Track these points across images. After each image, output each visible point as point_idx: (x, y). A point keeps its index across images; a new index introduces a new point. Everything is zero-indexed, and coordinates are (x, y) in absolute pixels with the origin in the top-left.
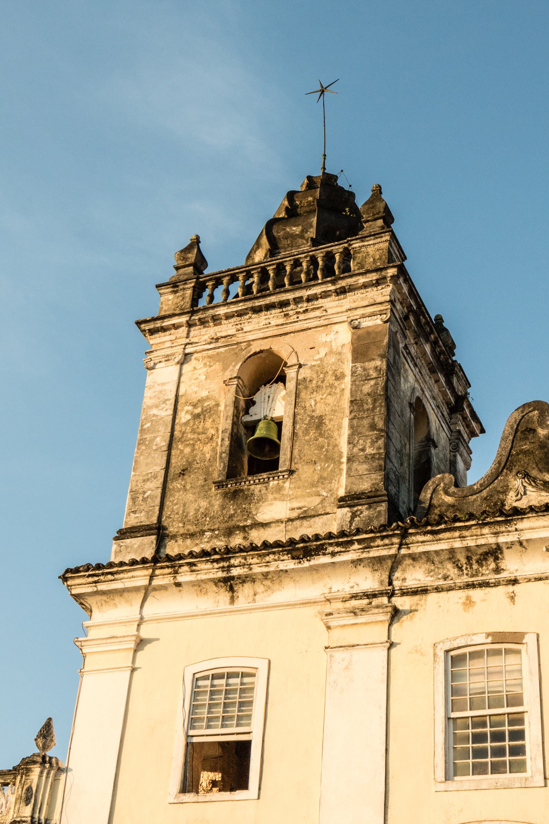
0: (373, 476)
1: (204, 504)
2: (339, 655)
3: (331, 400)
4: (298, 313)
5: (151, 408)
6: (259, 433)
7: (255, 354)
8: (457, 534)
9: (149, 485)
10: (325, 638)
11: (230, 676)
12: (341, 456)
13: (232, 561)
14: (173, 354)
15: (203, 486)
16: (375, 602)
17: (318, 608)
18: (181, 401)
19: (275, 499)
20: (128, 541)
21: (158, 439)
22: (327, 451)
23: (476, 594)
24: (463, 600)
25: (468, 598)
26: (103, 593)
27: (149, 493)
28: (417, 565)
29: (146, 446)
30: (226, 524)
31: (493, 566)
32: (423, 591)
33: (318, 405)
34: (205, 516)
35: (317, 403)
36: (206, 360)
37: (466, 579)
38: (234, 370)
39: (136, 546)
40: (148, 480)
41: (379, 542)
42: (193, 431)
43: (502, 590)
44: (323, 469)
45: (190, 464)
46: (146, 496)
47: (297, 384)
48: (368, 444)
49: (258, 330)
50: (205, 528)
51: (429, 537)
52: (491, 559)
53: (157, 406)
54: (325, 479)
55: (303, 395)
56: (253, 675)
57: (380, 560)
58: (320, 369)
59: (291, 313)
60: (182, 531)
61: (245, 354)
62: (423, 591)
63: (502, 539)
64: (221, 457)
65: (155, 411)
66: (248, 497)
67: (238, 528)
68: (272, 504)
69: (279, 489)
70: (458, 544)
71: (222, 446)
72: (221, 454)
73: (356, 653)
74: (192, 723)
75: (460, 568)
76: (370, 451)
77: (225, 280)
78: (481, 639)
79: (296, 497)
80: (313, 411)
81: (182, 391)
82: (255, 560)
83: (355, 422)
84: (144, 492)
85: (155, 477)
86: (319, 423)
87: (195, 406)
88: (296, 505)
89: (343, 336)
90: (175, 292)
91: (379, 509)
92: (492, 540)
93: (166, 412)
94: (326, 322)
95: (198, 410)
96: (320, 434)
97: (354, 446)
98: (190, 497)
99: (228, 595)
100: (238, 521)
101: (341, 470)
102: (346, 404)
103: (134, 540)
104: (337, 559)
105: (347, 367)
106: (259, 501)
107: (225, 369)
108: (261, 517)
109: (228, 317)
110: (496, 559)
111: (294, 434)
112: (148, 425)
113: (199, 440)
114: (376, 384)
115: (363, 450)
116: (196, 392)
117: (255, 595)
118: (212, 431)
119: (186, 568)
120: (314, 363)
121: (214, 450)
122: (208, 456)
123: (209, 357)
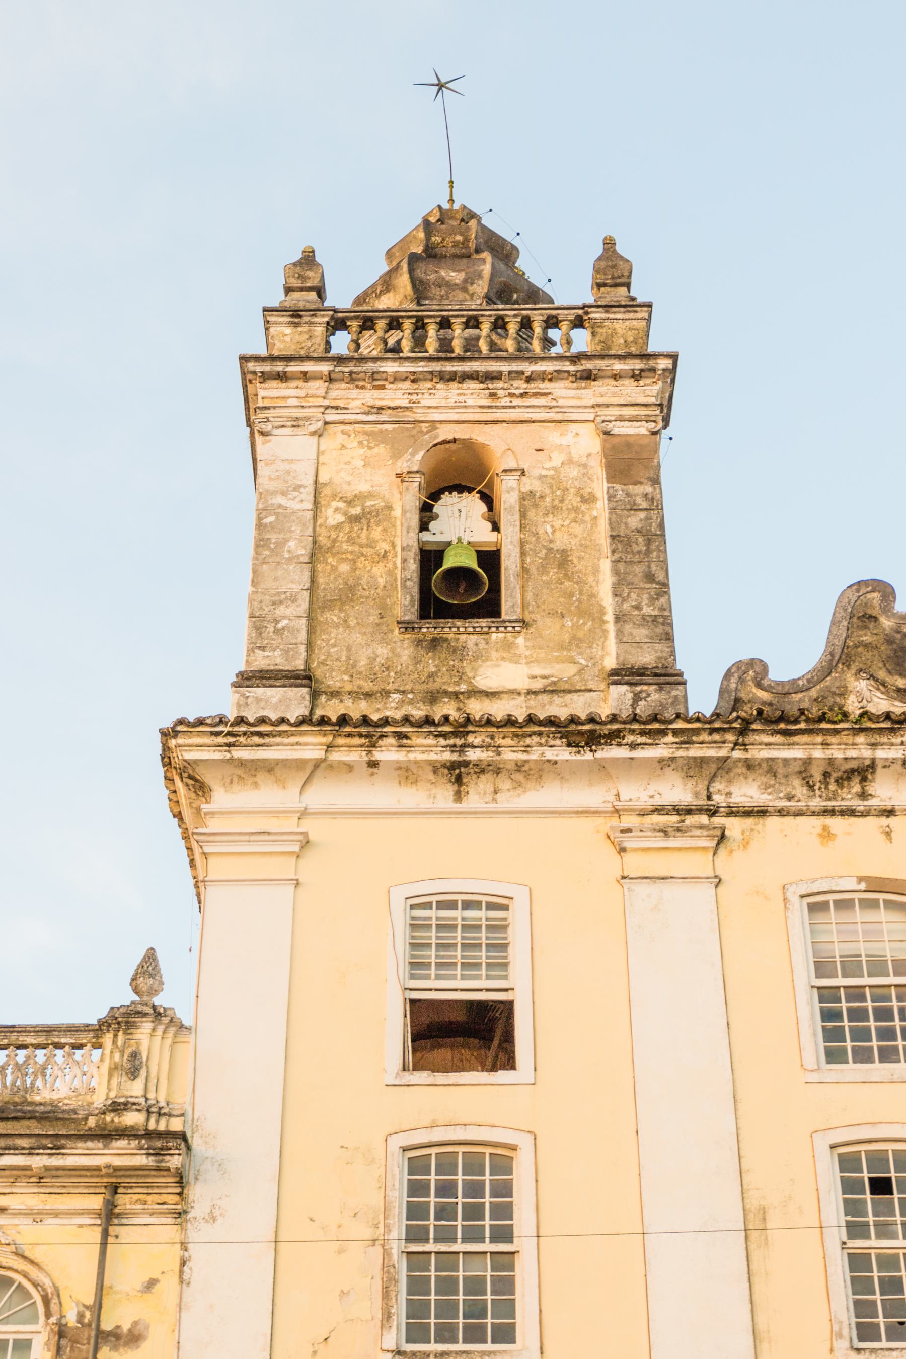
0: (658, 647)
1: (383, 652)
2: (643, 889)
3: (577, 529)
4: (511, 395)
5: (274, 493)
6: (450, 562)
7: (445, 442)
8: (819, 739)
10: (612, 864)
11: (467, 905)
12: (602, 611)
13: (471, 739)
14: (307, 419)
15: (378, 625)
16: (690, 820)
17: (599, 821)
18: (327, 491)
19: (503, 659)
20: (260, 691)
21: (292, 544)
22: (579, 600)
23: (836, 824)
24: (819, 830)
25: (825, 828)
26: (241, 763)
27: (284, 622)
28: (751, 776)
29: (272, 550)
30: (425, 686)
31: (857, 788)
32: (762, 813)
33: (558, 534)
34: (388, 669)
35: (558, 531)
36: (361, 438)
37: (817, 803)
38: (415, 460)
39: (274, 700)
40: (281, 602)
41: (704, 737)
42: (351, 540)
43: (872, 822)
44: (576, 626)
45: (352, 589)
46: (280, 626)
47: (523, 498)
48: (645, 602)
49: (451, 408)
50: (390, 687)
51: (778, 739)
52: (856, 780)
53: (284, 494)
54: (580, 640)
55: (531, 514)
56: (505, 908)
57: (701, 762)
58: (555, 481)
59: (501, 393)
60: (348, 687)
61: (428, 440)
62: (762, 813)
63: (880, 754)
64: (404, 586)
65: (279, 500)
66: (458, 652)
67: (446, 692)
68: (499, 666)
69: (508, 646)
70: (818, 753)
71: (403, 569)
72: (404, 581)
73: (667, 888)
74: (417, 966)
75: (811, 787)
76: (647, 610)
77: (381, 324)
78: (851, 884)
79: (537, 661)
80: (551, 541)
81: (322, 479)
82: (508, 742)
83: (621, 566)
84: (277, 621)
85: (293, 599)
86: (563, 560)
87: (350, 503)
88: (538, 671)
89: (586, 443)
90: (297, 325)
91: (674, 693)
92: (867, 753)
93: (302, 503)
94: (559, 417)
95: (357, 511)
96: (566, 575)
97: (624, 600)
98: (357, 638)
99: (451, 789)
100: (444, 683)
101: (605, 632)
102: (604, 541)
103: (270, 691)
104: (639, 753)
105: (600, 486)
106: (476, 658)
107: (396, 456)
108: (482, 682)
109: (397, 378)
110: (864, 779)
111: (525, 570)
112: (271, 519)
113: (363, 555)
114: (648, 518)
115: (638, 607)
116: (349, 483)
117: (496, 792)
118: (384, 546)
119: (391, 741)
120: (544, 472)
121: (390, 573)
122: (381, 582)
123: (366, 433)
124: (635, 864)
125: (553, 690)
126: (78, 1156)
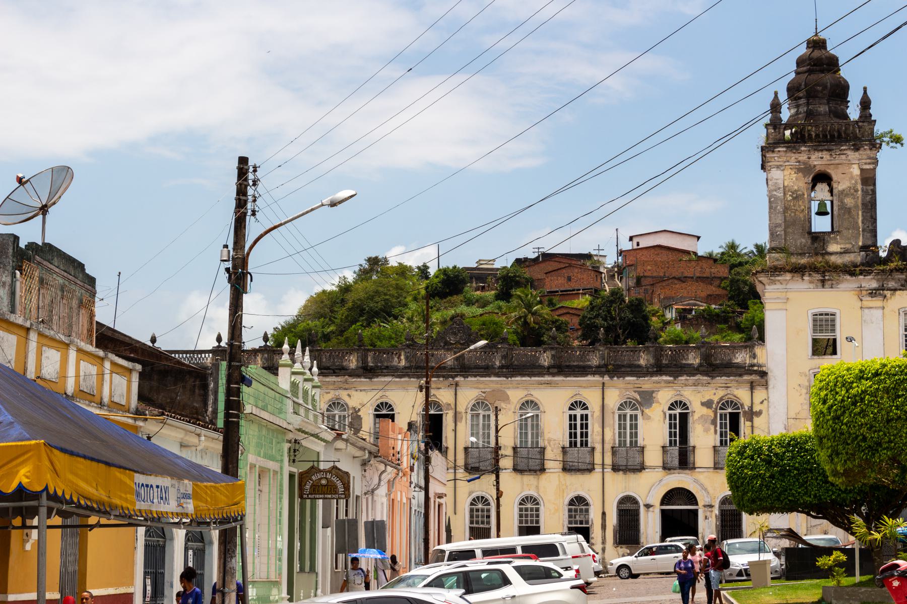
1: (803, 241)
2: (866, 311)
9: (778, 229)
10: (859, 304)
49: (819, 160)
86: (849, 211)
102: (860, 205)
105: (859, 187)
124: (865, 303)
125: (846, 252)
126: (746, 377)
